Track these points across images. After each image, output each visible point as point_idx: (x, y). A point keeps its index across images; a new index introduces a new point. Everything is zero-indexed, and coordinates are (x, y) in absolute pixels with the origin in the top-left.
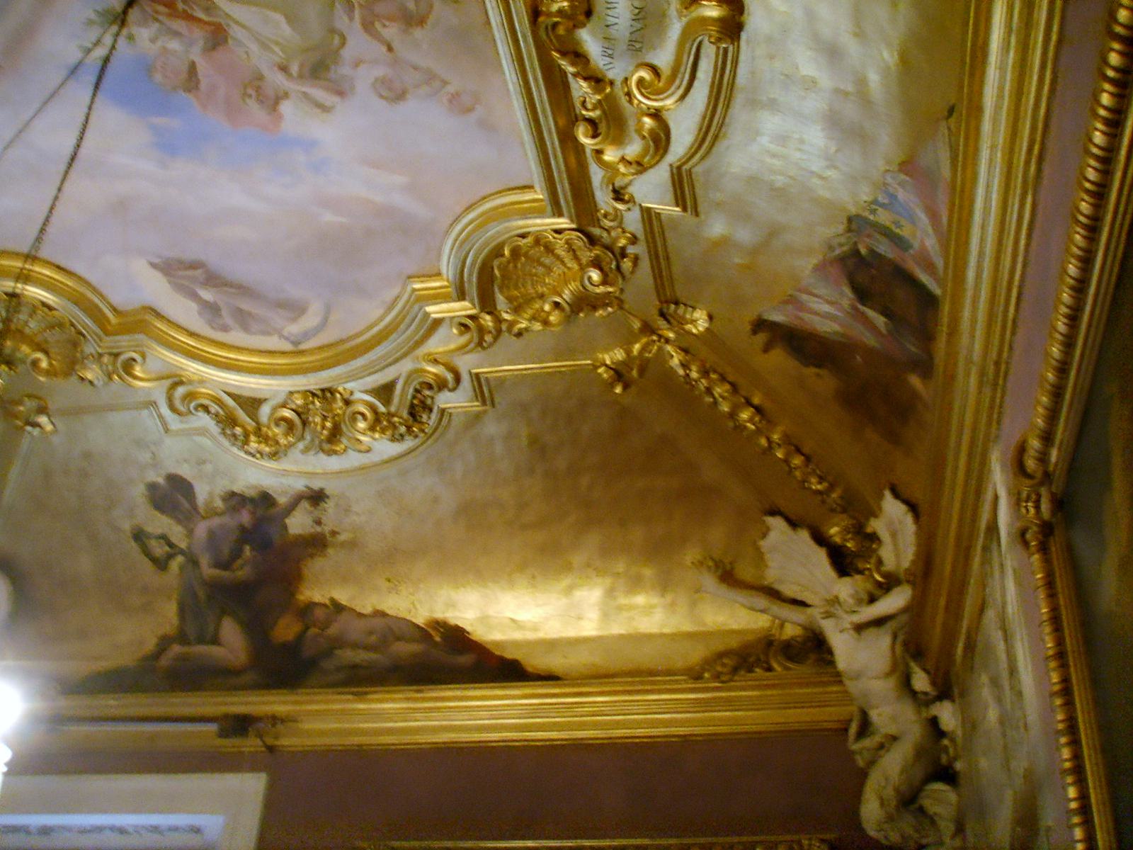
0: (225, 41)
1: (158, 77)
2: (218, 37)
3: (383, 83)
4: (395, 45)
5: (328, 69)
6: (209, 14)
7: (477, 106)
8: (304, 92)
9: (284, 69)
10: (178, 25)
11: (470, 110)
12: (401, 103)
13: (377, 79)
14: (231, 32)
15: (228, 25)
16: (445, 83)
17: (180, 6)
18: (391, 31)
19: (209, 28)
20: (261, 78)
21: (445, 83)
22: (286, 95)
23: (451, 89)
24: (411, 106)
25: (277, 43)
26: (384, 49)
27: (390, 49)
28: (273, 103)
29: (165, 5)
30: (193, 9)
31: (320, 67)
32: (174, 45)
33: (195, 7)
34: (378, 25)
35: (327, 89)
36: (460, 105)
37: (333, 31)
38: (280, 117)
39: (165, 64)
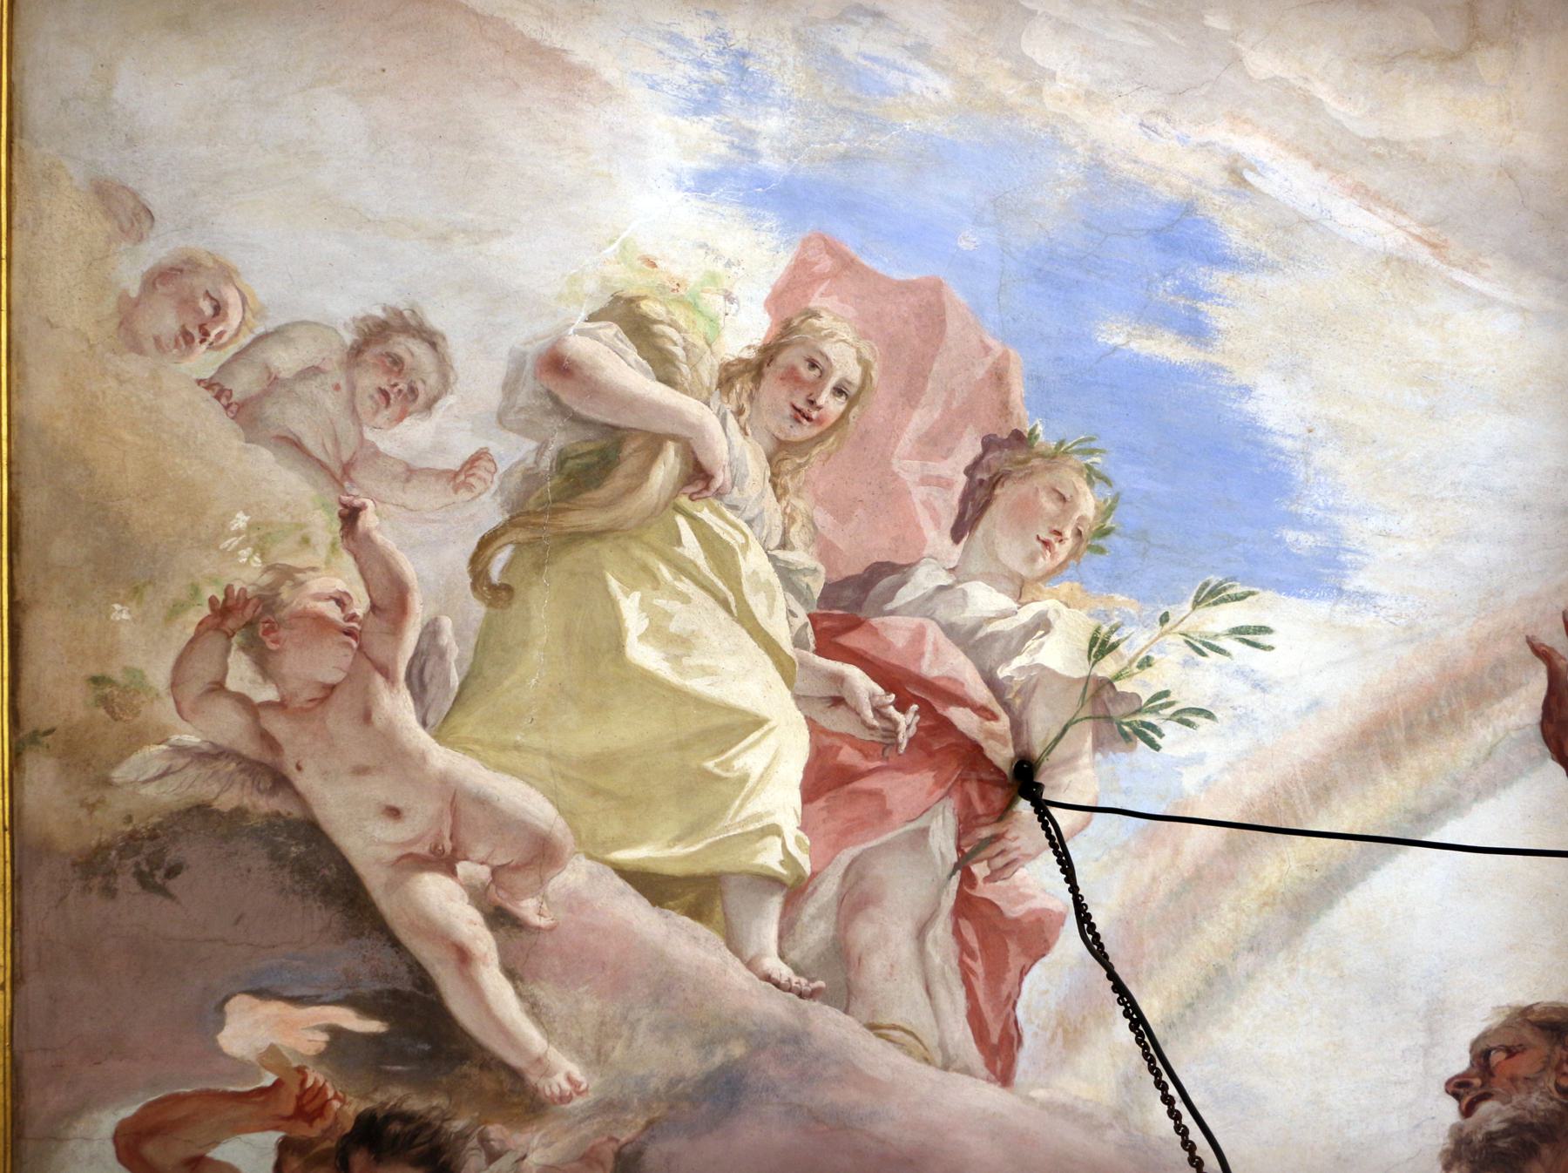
0: (831, 591)
1: (1088, 504)
2: (843, 616)
3: (413, 391)
4: (325, 526)
5: (562, 459)
6: (839, 679)
7: (134, 291)
8: (669, 381)
9: (698, 475)
10: (947, 663)
11: (163, 277)
12: (378, 313)
13: (429, 406)
14: (802, 618)
15: (798, 642)
16: (215, 387)
17: (907, 722)
18: (333, 580)
19: (853, 640)
20: (780, 453)
21: (215, 387)
22: (727, 377)
23: (203, 361)
24: (346, 306)
25: (683, 568)
26: (369, 520)
27: (350, 516)
28: (778, 366)
29: (947, 725)
30: (878, 711)
31: (588, 472)
32: (985, 601)
33: (869, 714)
34: (360, 606)
35: (593, 387)
36: (190, 296)
37: (498, 594)
38: (775, 302)
39: (1046, 543)
